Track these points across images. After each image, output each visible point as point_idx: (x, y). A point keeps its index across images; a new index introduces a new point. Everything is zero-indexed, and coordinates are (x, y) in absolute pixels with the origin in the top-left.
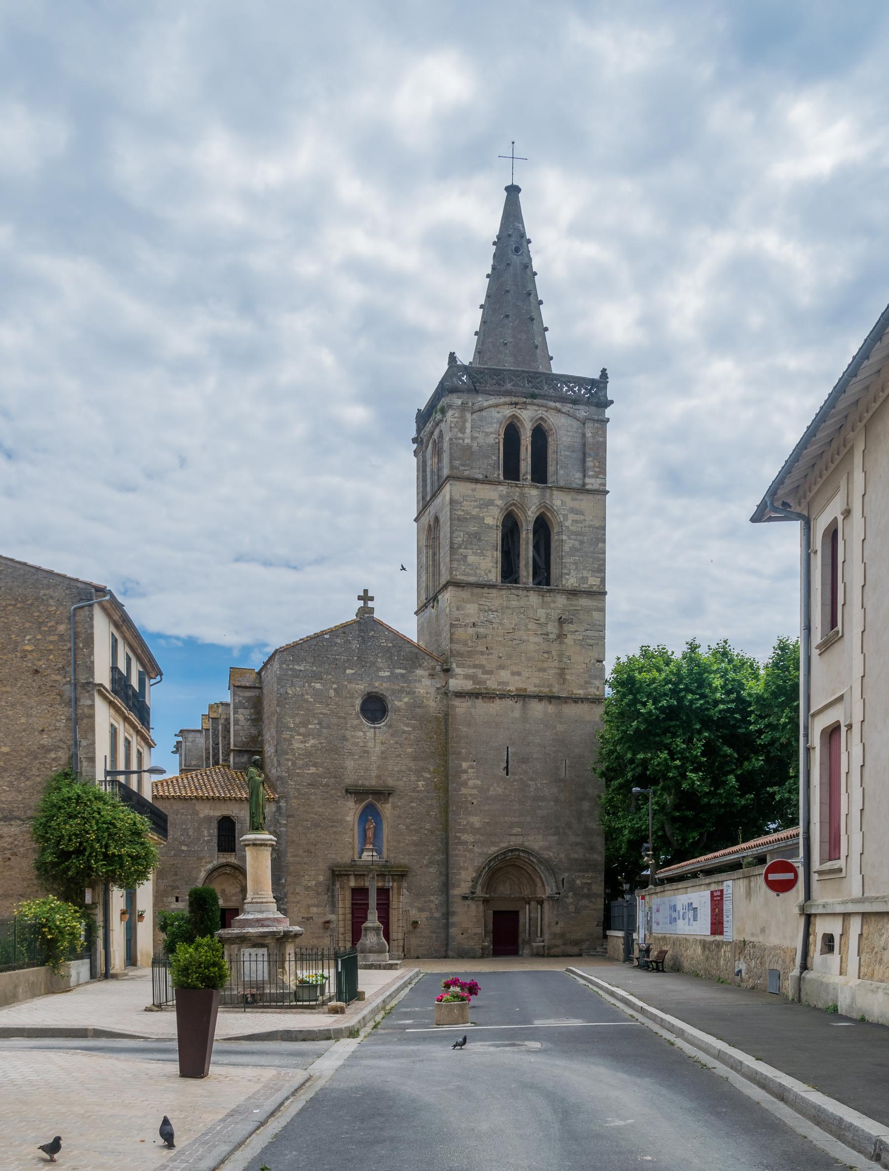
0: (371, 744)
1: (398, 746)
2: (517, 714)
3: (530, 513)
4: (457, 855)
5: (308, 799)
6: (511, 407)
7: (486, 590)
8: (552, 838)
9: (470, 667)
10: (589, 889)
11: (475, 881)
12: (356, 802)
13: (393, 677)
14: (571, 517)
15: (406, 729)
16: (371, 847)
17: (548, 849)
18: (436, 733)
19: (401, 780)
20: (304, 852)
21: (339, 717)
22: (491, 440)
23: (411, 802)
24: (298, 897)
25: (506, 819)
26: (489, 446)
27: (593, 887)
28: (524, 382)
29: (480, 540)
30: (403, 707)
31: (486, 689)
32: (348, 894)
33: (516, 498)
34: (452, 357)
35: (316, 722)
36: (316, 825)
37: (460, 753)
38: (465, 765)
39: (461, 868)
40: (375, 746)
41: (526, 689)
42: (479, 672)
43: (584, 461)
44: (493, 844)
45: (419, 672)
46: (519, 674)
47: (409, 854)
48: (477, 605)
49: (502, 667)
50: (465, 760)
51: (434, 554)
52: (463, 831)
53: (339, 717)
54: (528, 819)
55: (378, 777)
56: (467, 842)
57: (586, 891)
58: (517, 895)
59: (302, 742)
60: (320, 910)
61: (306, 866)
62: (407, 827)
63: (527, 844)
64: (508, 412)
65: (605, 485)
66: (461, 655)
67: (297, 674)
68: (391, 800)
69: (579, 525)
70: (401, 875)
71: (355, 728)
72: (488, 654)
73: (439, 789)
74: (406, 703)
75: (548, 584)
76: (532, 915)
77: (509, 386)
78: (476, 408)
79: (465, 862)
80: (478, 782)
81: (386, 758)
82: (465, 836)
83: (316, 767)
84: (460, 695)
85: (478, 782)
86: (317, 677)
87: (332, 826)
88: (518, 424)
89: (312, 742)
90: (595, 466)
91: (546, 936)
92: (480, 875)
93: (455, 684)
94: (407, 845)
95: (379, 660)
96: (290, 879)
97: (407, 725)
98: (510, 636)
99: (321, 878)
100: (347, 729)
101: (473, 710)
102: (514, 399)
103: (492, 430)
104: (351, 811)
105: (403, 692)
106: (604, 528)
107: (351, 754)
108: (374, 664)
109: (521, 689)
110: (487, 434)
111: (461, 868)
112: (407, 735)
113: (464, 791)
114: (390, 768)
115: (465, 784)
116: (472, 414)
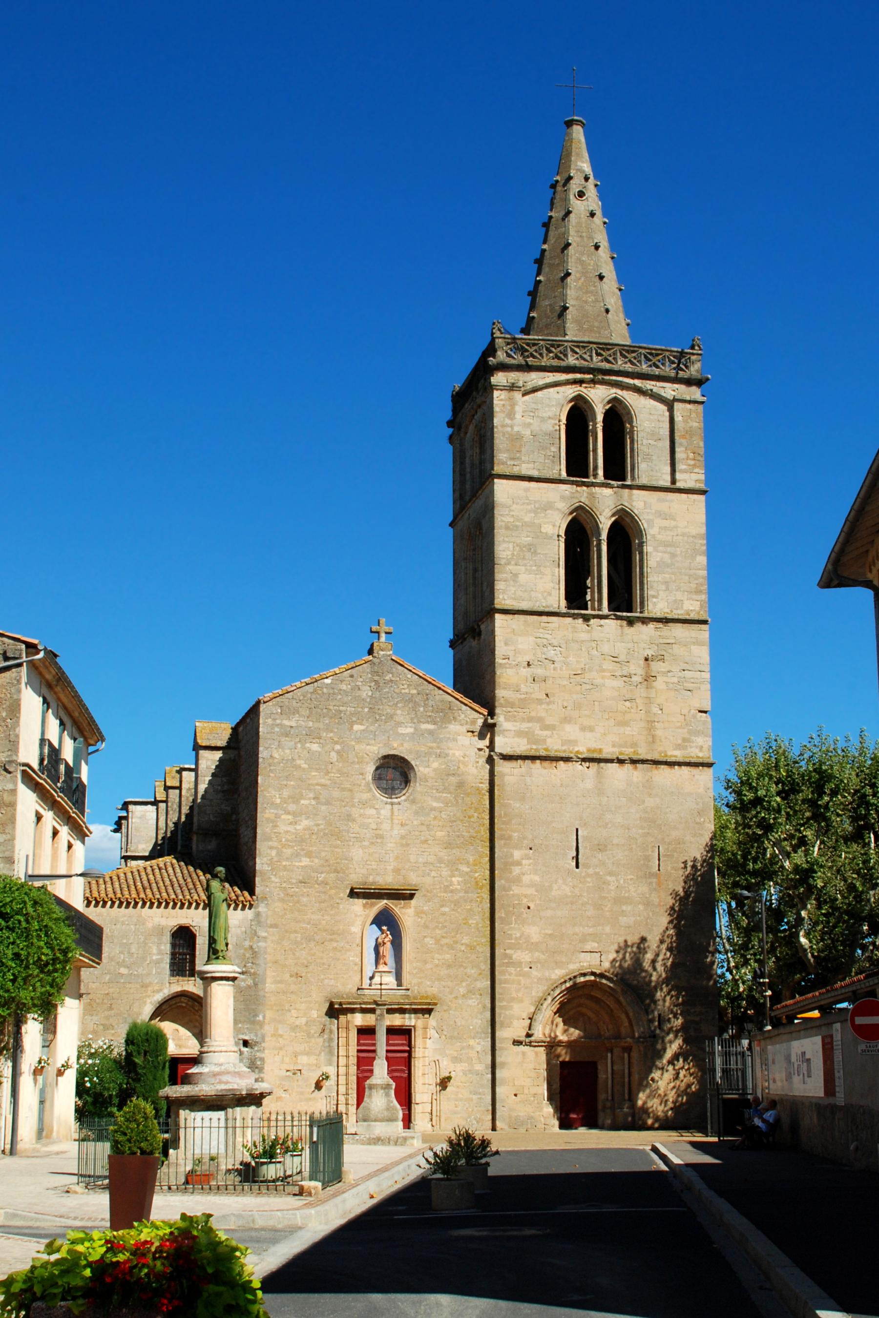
0: (386, 826)
2: (589, 784)
4: (506, 982)
5: (298, 902)
7: (544, 618)
9: (523, 720)
12: (364, 906)
13: (418, 734)
15: (435, 804)
18: (476, 809)
19: (429, 875)
20: (291, 976)
21: (343, 790)
22: (549, 426)
23: (442, 906)
24: (280, 1040)
25: (577, 929)
26: (546, 434)
28: (591, 356)
29: (535, 553)
30: (432, 774)
31: (546, 750)
32: (353, 1034)
35: (311, 795)
36: (309, 939)
37: (510, 838)
38: (517, 854)
40: (392, 829)
41: (600, 751)
42: (536, 727)
44: (558, 964)
45: (453, 727)
46: (591, 729)
47: (439, 979)
48: (532, 639)
49: (567, 720)
50: (518, 847)
51: (475, 570)
52: (515, 947)
53: (343, 790)
55: (397, 871)
56: (521, 963)
59: (291, 823)
60: (312, 1060)
61: (293, 997)
62: (437, 941)
64: (571, 391)
66: (512, 705)
69: (668, 533)
71: (364, 804)
72: (548, 704)
73: (481, 888)
74: (435, 770)
76: (615, 1068)
77: (572, 360)
80: (537, 878)
81: (407, 845)
82: (519, 953)
83: (310, 857)
85: (537, 878)
86: (312, 735)
87: (331, 940)
88: (584, 406)
90: (688, 458)
93: (503, 744)
94: (437, 966)
95: (399, 712)
96: (269, 1014)
97: (437, 799)
99: (314, 1014)
100: (353, 806)
101: (528, 779)
102: (578, 376)
103: (550, 414)
108: (391, 717)
109: (594, 751)
110: (543, 420)
113: (516, 890)
114: (412, 858)
115: (517, 880)
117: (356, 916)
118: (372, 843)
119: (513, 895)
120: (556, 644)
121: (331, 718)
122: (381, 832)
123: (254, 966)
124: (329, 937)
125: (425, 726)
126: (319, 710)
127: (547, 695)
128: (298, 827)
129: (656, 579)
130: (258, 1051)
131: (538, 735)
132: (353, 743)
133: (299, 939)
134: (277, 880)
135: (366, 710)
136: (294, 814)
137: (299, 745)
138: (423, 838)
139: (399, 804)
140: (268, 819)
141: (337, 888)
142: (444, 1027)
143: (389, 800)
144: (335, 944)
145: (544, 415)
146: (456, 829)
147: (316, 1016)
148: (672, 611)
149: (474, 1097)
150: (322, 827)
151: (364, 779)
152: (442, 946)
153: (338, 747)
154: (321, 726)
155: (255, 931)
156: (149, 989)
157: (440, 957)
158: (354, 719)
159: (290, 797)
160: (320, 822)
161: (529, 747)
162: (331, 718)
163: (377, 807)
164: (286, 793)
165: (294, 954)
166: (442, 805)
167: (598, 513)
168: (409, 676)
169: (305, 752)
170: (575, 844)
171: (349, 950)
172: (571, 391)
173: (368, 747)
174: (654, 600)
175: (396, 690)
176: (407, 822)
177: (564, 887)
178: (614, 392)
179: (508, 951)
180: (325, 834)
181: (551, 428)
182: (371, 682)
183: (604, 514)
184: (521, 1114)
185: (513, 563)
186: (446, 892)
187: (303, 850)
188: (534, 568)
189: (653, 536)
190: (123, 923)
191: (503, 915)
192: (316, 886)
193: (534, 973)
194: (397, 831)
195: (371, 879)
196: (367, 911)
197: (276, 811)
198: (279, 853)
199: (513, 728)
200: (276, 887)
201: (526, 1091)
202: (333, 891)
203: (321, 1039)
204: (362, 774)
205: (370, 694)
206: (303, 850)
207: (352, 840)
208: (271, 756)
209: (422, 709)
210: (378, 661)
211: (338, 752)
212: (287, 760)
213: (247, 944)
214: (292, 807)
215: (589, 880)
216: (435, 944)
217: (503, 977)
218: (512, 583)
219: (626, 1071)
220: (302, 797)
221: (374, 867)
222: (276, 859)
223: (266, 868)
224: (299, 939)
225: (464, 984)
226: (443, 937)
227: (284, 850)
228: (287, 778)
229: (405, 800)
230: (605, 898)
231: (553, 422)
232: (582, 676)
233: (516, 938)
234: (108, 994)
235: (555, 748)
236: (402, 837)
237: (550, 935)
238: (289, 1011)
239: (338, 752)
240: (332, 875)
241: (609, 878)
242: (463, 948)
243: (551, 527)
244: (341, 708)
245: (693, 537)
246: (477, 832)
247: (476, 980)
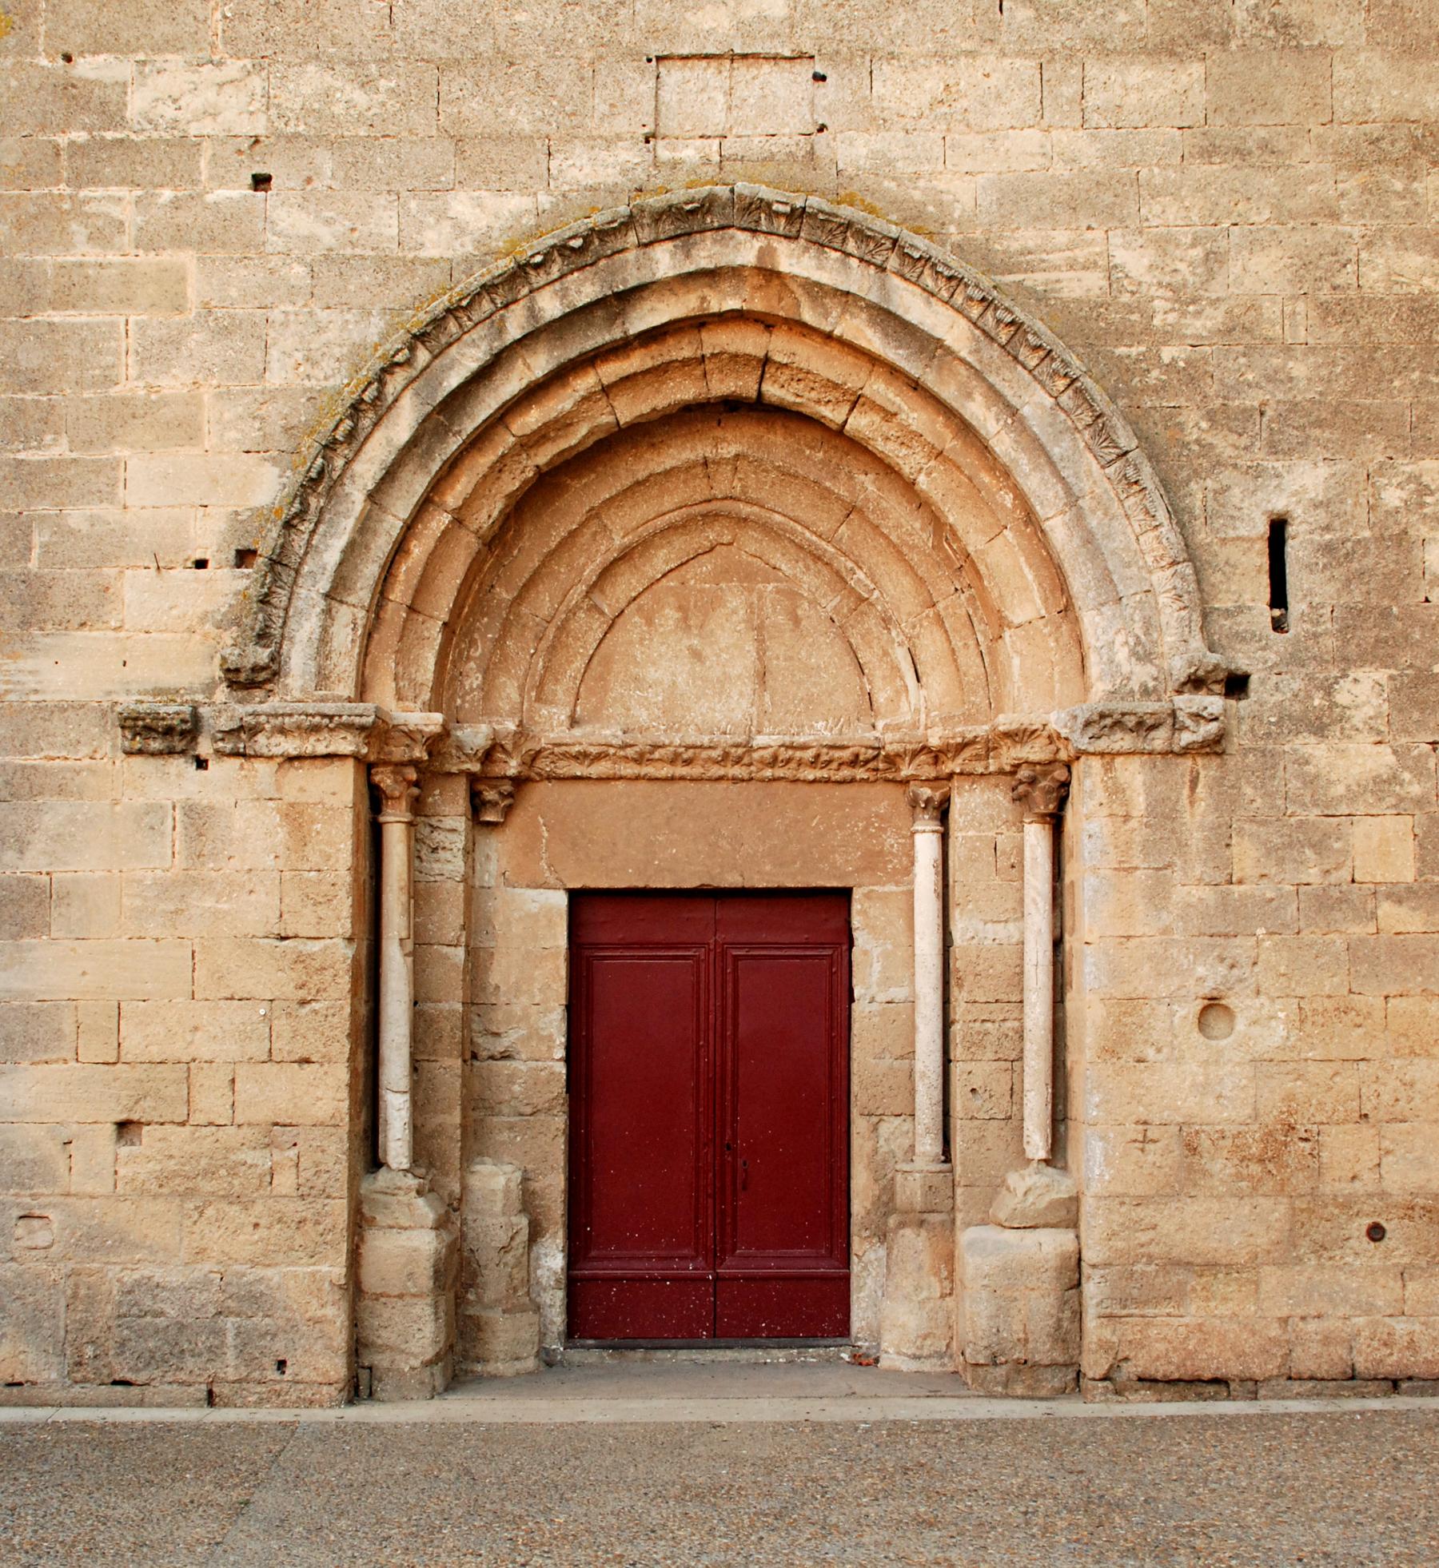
4: (72, 289)
17: (1101, 199)
39: (122, 417)
44: (473, 153)
56: (186, 145)
63: (852, 150)
79: (161, 351)
111: (122, 417)
179: (86, 67)
193: (287, 216)
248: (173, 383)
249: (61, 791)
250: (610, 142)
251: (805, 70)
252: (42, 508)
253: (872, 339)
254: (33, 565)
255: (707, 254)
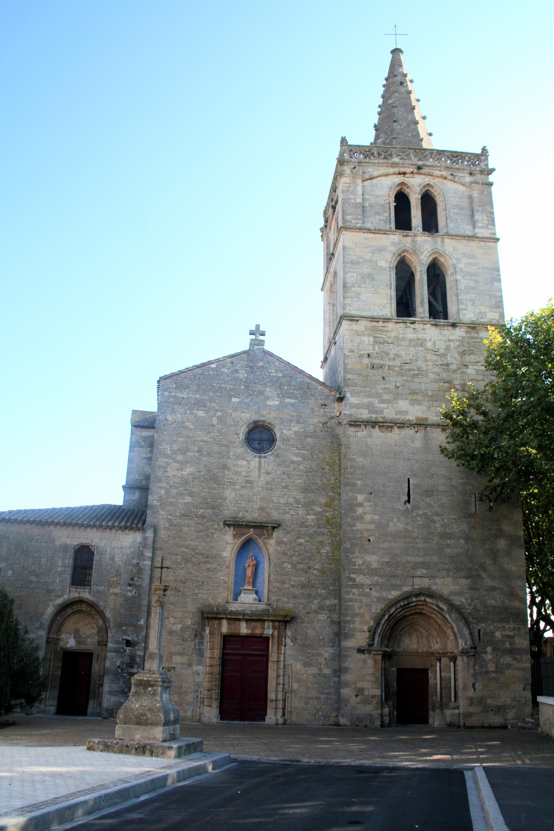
1: (286, 477)
3: (422, 257)
5: (180, 531)
6: (399, 176)
8: (464, 581)
10: (511, 643)
11: (373, 632)
12: (234, 536)
14: (464, 260)
15: (295, 459)
16: (250, 588)
18: (328, 464)
21: (221, 445)
23: (299, 538)
27: (517, 640)
29: (373, 279)
31: (384, 418)
33: (408, 245)
34: (343, 141)
35: (196, 449)
36: (187, 561)
37: (355, 485)
38: (360, 498)
39: (356, 615)
40: (259, 476)
43: (472, 216)
44: (394, 587)
47: (295, 597)
50: (360, 492)
52: (359, 572)
53: (221, 445)
54: (435, 559)
57: (507, 645)
58: (425, 650)
59: (178, 470)
60: (184, 659)
61: (172, 607)
62: (294, 566)
64: (398, 179)
65: (495, 234)
67: (179, 402)
68: (275, 534)
70: (285, 621)
71: (238, 457)
74: (296, 433)
75: (446, 317)
78: (367, 177)
79: (360, 607)
80: (376, 517)
83: (191, 496)
84: (355, 424)
85: (376, 517)
86: (200, 404)
87: (206, 562)
89: (188, 470)
90: (483, 220)
91: (462, 702)
92: (378, 624)
94: (293, 586)
97: (296, 455)
98: (407, 366)
99: (189, 622)
100: (228, 458)
104: (228, 544)
105: (291, 421)
106: (498, 270)
107: (232, 483)
108: (262, 393)
109: (422, 419)
112: (296, 466)
115: (361, 518)
116: (363, 181)
117: (227, 543)
118: (243, 487)
119: (357, 530)
120: (390, 341)
121: (214, 392)
122: (250, 479)
123: (139, 580)
124: (204, 560)
125: (287, 400)
126: (205, 387)
127: (383, 378)
128: (183, 473)
129: (465, 297)
130: (138, 650)
131: (377, 407)
132: (231, 411)
133: (179, 560)
134: (164, 513)
135: (242, 387)
136: (181, 462)
137: (188, 412)
138: (284, 484)
139: (265, 457)
140: (160, 466)
141: (212, 520)
142: (298, 637)
143: (258, 455)
144: (209, 566)
145: (378, 194)
146: (311, 478)
147: (189, 623)
148: (478, 320)
149: (322, 696)
150: (203, 473)
151: (239, 438)
152: (298, 570)
153: (219, 414)
154: (206, 398)
155: (142, 552)
156: (53, 594)
157: (296, 579)
158: (232, 394)
159: (178, 450)
160: (202, 469)
161: (370, 415)
162: (214, 392)
163: (248, 459)
164: (175, 447)
165: (174, 573)
166: (300, 459)
167: (419, 254)
168: (277, 364)
169: (193, 417)
170: (406, 490)
171: (220, 571)
172: (398, 179)
173: (243, 414)
174: (464, 312)
175: (267, 374)
176: (272, 471)
177: (399, 524)
178: (427, 180)
179: (352, 576)
180: (204, 478)
181: (383, 202)
182: (247, 367)
183: (424, 254)
184: (362, 712)
185: (356, 286)
186: (302, 527)
187: (187, 490)
188: (372, 289)
189: (461, 269)
190: (37, 541)
191: (348, 546)
192: (196, 519)
193: (374, 593)
194: (264, 478)
195: (241, 514)
196: (237, 540)
197: (166, 460)
198: (167, 492)
199: (357, 402)
200: (163, 519)
201: (366, 693)
202: (209, 524)
203: (193, 643)
204: (237, 434)
205: (246, 375)
206: (187, 490)
207: (226, 483)
208: (166, 419)
209: (286, 388)
210: (253, 352)
211: (218, 418)
212: (178, 422)
213: (135, 561)
214: (180, 457)
215: (419, 519)
216: (292, 568)
217: (348, 597)
218: (356, 299)
219: (452, 677)
220: (188, 450)
221: (243, 505)
222: (164, 497)
223: (156, 503)
224: (179, 560)
225: (315, 602)
226: (298, 563)
227: (172, 490)
228: (178, 435)
229: (271, 455)
230: (432, 533)
231: (385, 198)
232: (411, 365)
233: (359, 564)
234: (19, 596)
235: (390, 417)
236: (267, 483)
237: (387, 563)
238: (168, 618)
239: (218, 418)
240: (208, 510)
241: (435, 518)
242: (315, 572)
243: (384, 262)
244: (223, 385)
245: (491, 270)
246: (329, 480)
247: (326, 598)
248: (361, 611)
249: (349, 657)
250: (408, 586)
251: (429, 579)
252: (347, 625)
253: (436, 608)
254: (346, 631)
255: (419, 599)
